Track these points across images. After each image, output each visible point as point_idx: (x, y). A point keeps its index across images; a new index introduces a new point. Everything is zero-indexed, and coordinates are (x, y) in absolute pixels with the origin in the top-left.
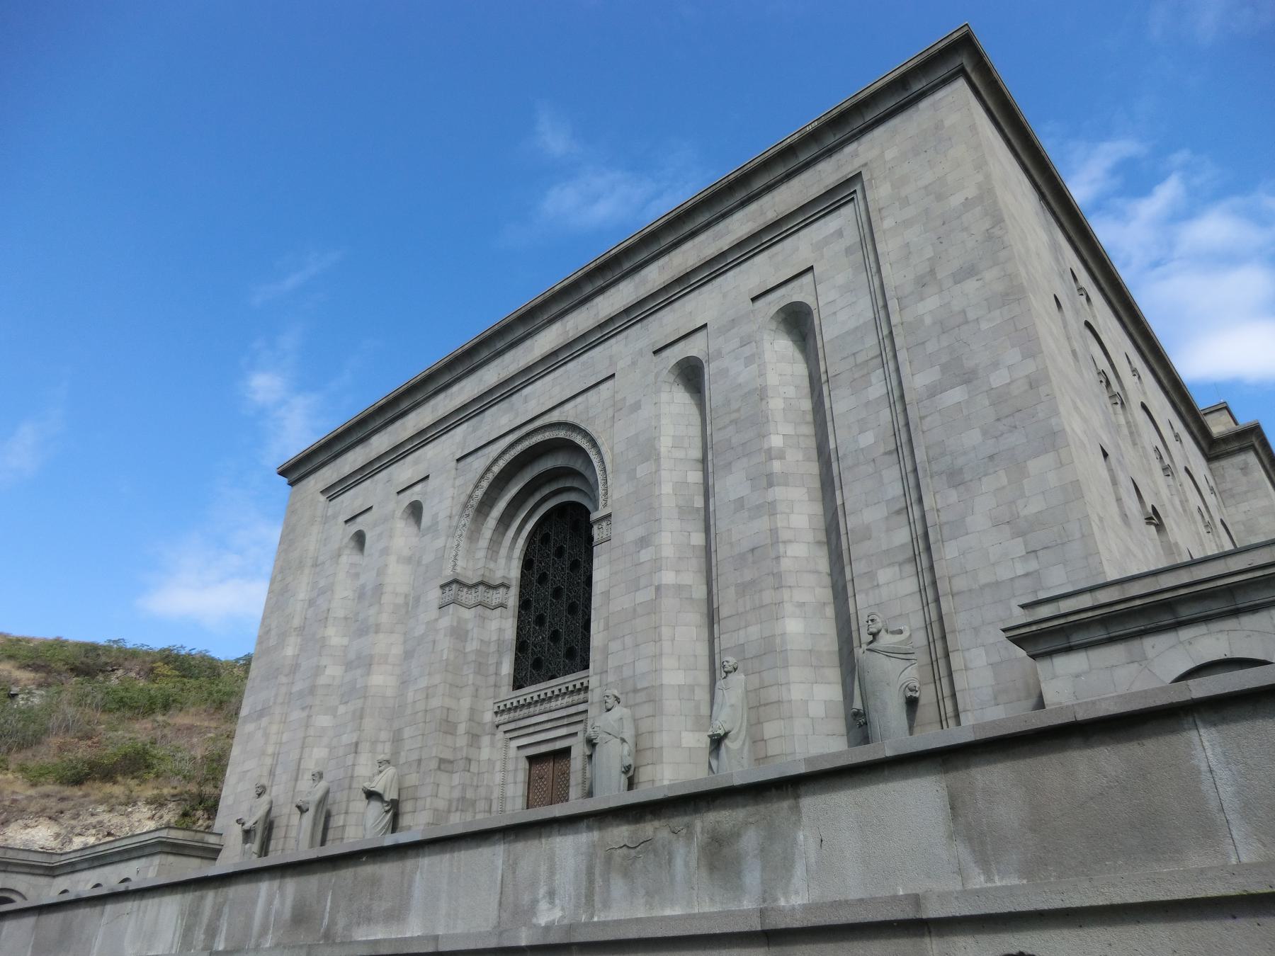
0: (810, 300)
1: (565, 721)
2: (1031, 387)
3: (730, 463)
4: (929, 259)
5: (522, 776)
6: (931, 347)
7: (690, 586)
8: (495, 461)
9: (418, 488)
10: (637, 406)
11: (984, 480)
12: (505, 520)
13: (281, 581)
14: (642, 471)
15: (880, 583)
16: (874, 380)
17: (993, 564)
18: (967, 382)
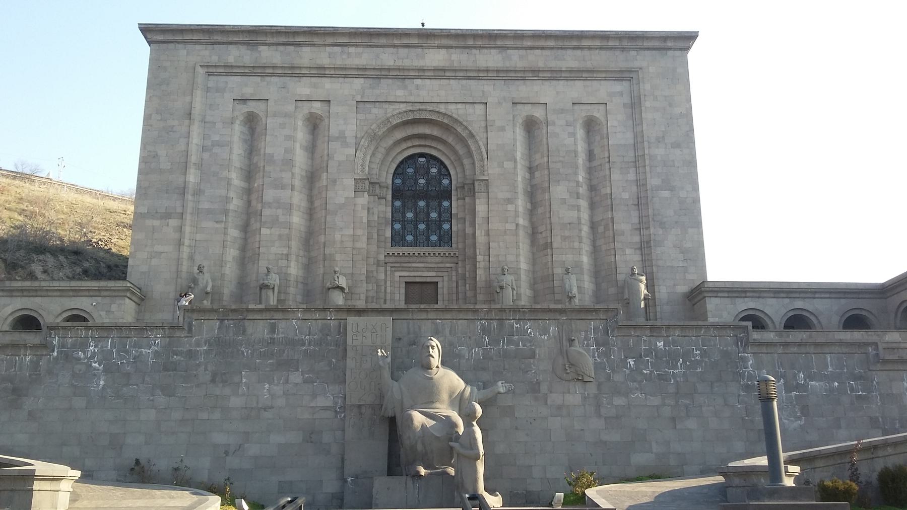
0: (603, 119)
2: (694, 203)
3: (559, 181)
4: (663, 131)
5: (403, 291)
6: (659, 170)
7: (527, 227)
8: (393, 116)
9: (317, 105)
10: (502, 129)
11: (673, 229)
12: (389, 150)
13: (161, 120)
14: (508, 165)
15: (627, 253)
16: (631, 171)
17: (673, 260)
18: (672, 191)
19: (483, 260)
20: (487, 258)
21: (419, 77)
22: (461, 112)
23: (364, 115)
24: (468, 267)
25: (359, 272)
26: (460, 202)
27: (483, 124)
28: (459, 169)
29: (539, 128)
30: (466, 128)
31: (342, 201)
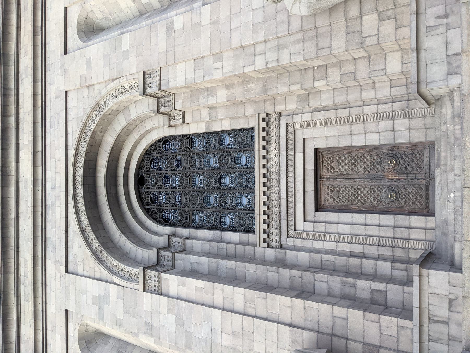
1: (291, 153)
5: (333, 216)
8: (80, 223)
10: (89, 62)
19: (263, 56)
20: (260, 48)
21: (44, 185)
22: (75, 128)
23: (79, 263)
24: (283, 89)
25: (289, 310)
26: (188, 119)
27: (86, 91)
28: (149, 125)
29: (92, 11)
30: (89, 117)
31: (172, 318)
